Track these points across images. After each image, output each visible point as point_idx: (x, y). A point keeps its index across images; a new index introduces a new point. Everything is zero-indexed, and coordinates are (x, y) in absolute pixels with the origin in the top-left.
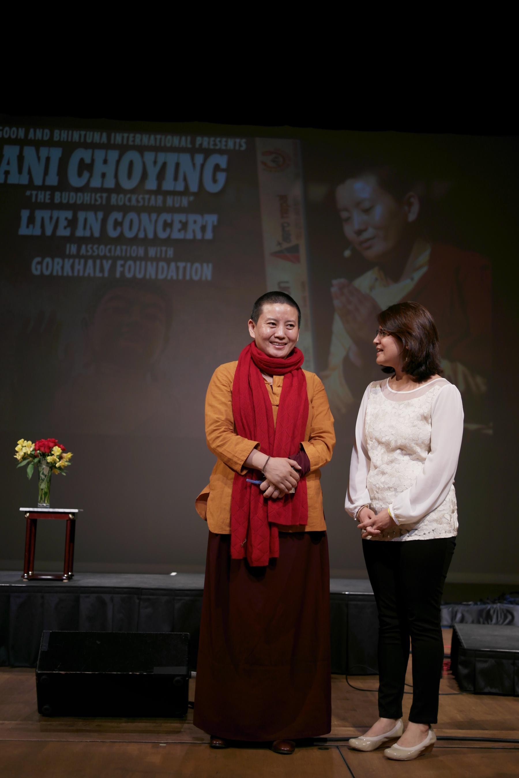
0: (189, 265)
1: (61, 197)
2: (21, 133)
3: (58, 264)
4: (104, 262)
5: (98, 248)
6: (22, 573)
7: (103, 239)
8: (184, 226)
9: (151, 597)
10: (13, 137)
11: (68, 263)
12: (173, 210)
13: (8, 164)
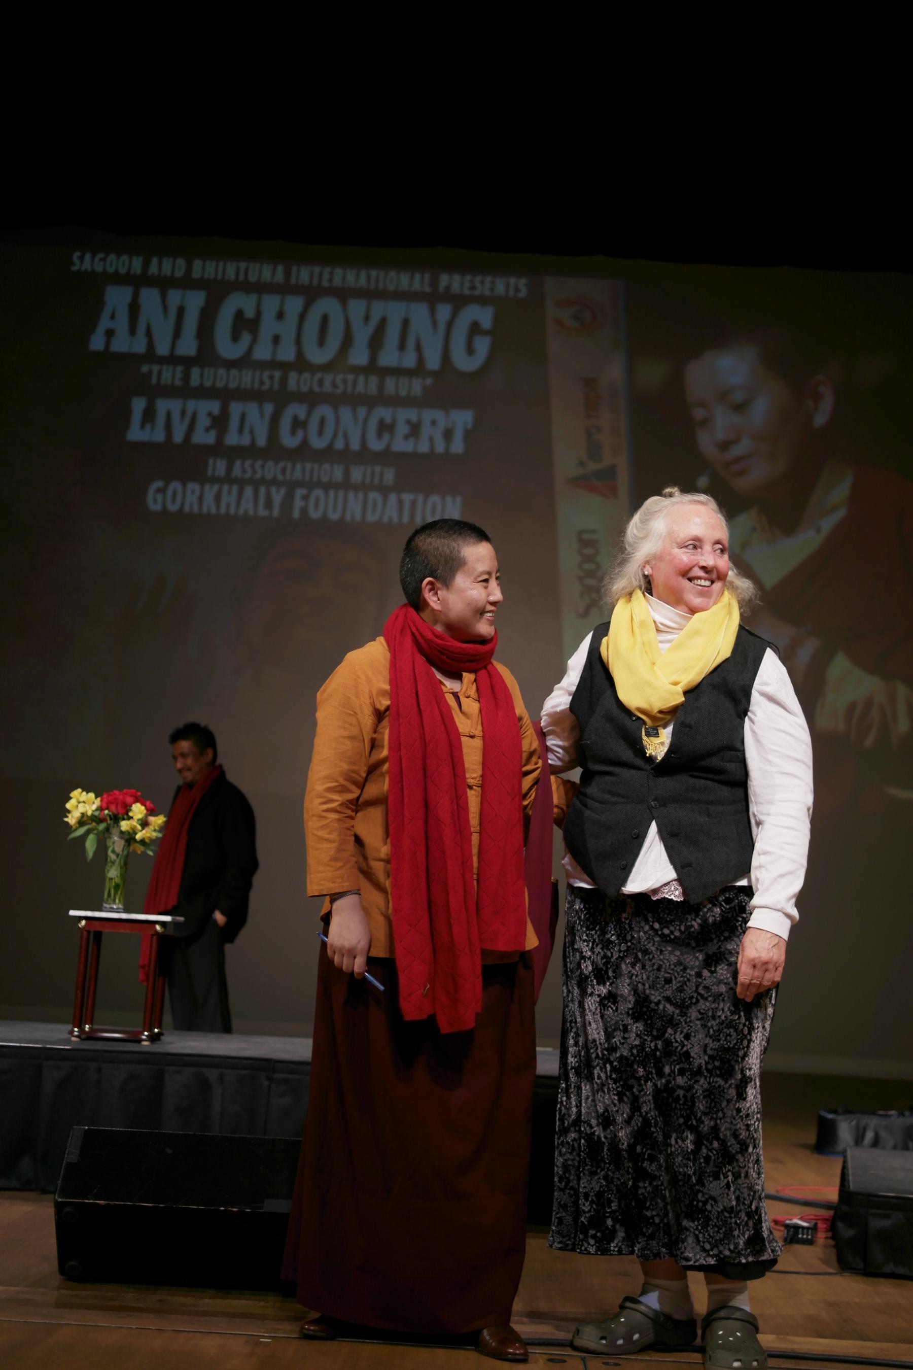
0: (421, 498)
1: (202, 376)
2: (137, 265)
3: (193, 492)
4: (273, 490)
5: (263, 467)
6: (70, 1027)
7: (273, 450)
8: (415, 429)
9: (290, 1076)
10: (123, 271)
11: (210, 492)
12: (396, 402)
13: (113, 317)
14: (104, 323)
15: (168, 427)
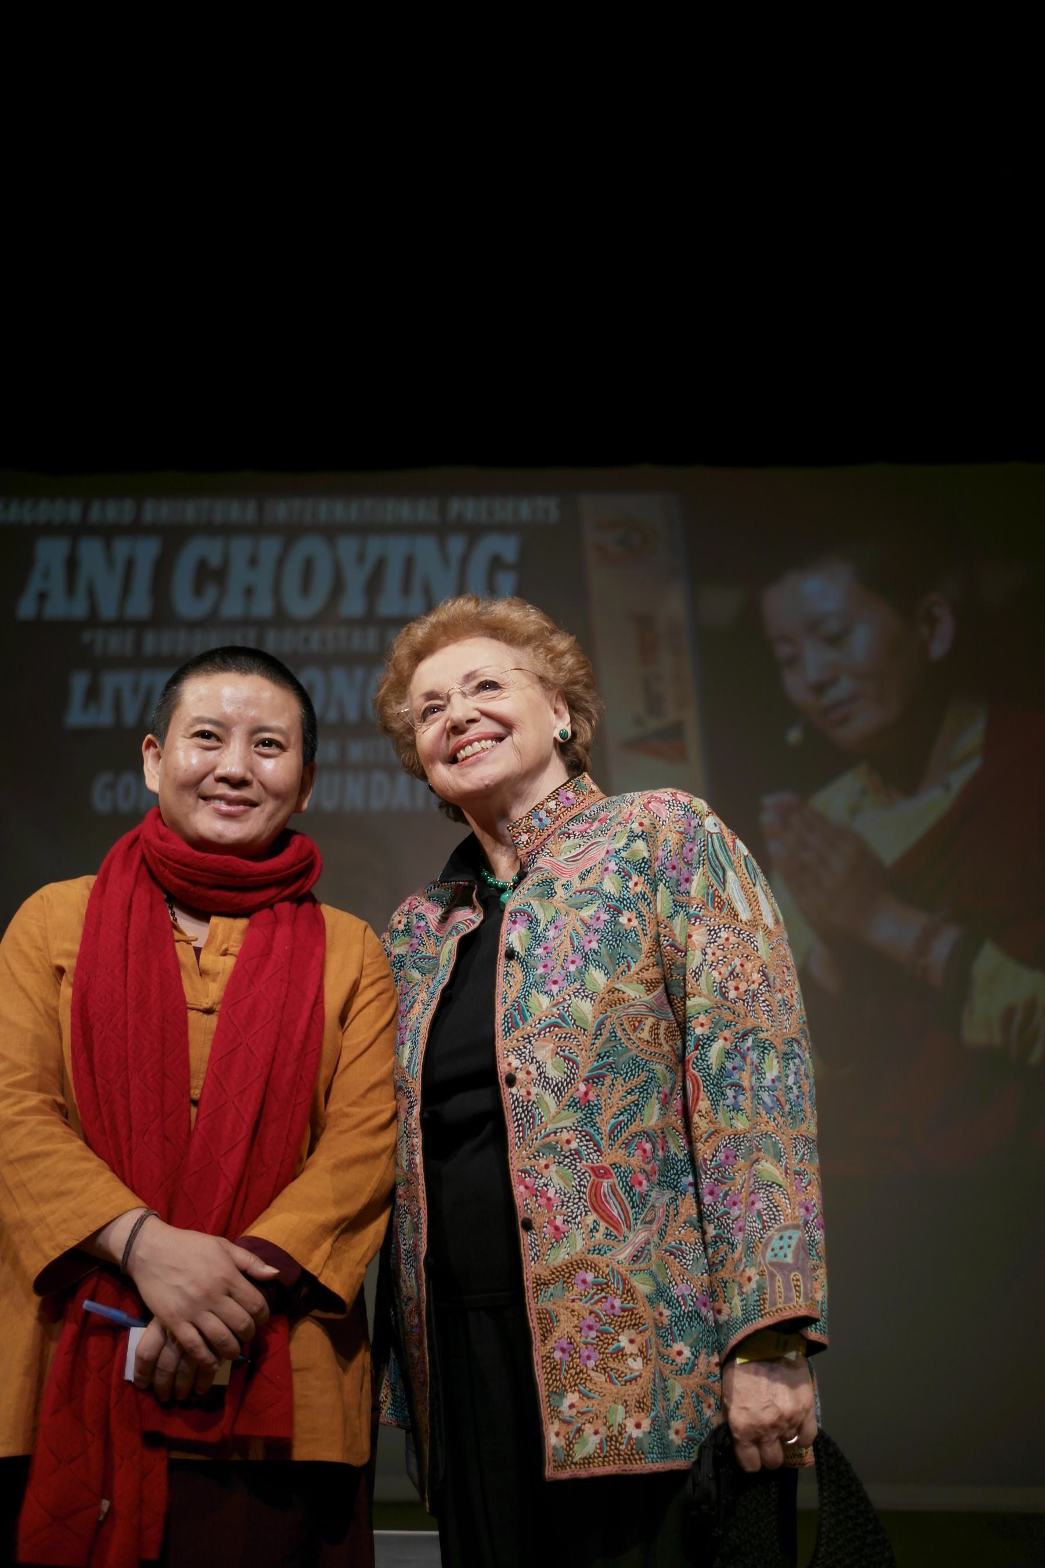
2: (74, 511)
14: (35, 584)
15: (118, 707)
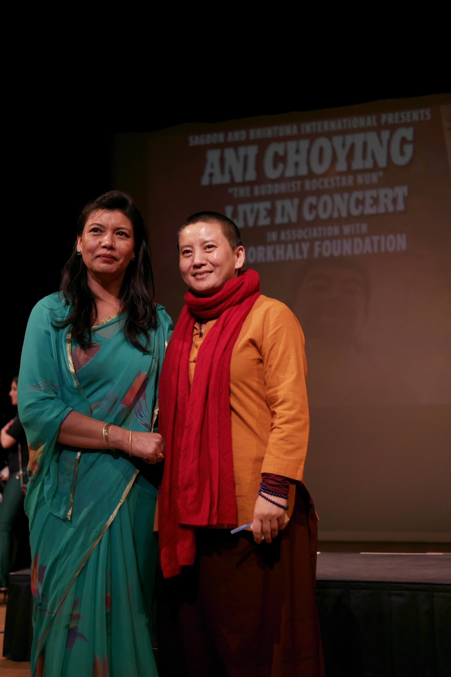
0: (383, 238)
7: (301, 223)
8: (376, 201)
10: (215, 142)
11: (270, 249)
12: (364, 187)
14: (208, 170)
15: (245, 219)
